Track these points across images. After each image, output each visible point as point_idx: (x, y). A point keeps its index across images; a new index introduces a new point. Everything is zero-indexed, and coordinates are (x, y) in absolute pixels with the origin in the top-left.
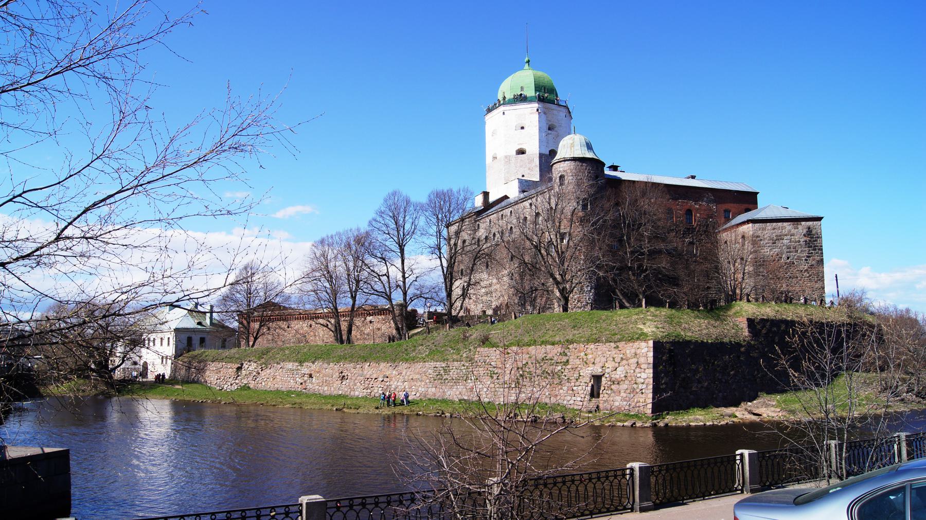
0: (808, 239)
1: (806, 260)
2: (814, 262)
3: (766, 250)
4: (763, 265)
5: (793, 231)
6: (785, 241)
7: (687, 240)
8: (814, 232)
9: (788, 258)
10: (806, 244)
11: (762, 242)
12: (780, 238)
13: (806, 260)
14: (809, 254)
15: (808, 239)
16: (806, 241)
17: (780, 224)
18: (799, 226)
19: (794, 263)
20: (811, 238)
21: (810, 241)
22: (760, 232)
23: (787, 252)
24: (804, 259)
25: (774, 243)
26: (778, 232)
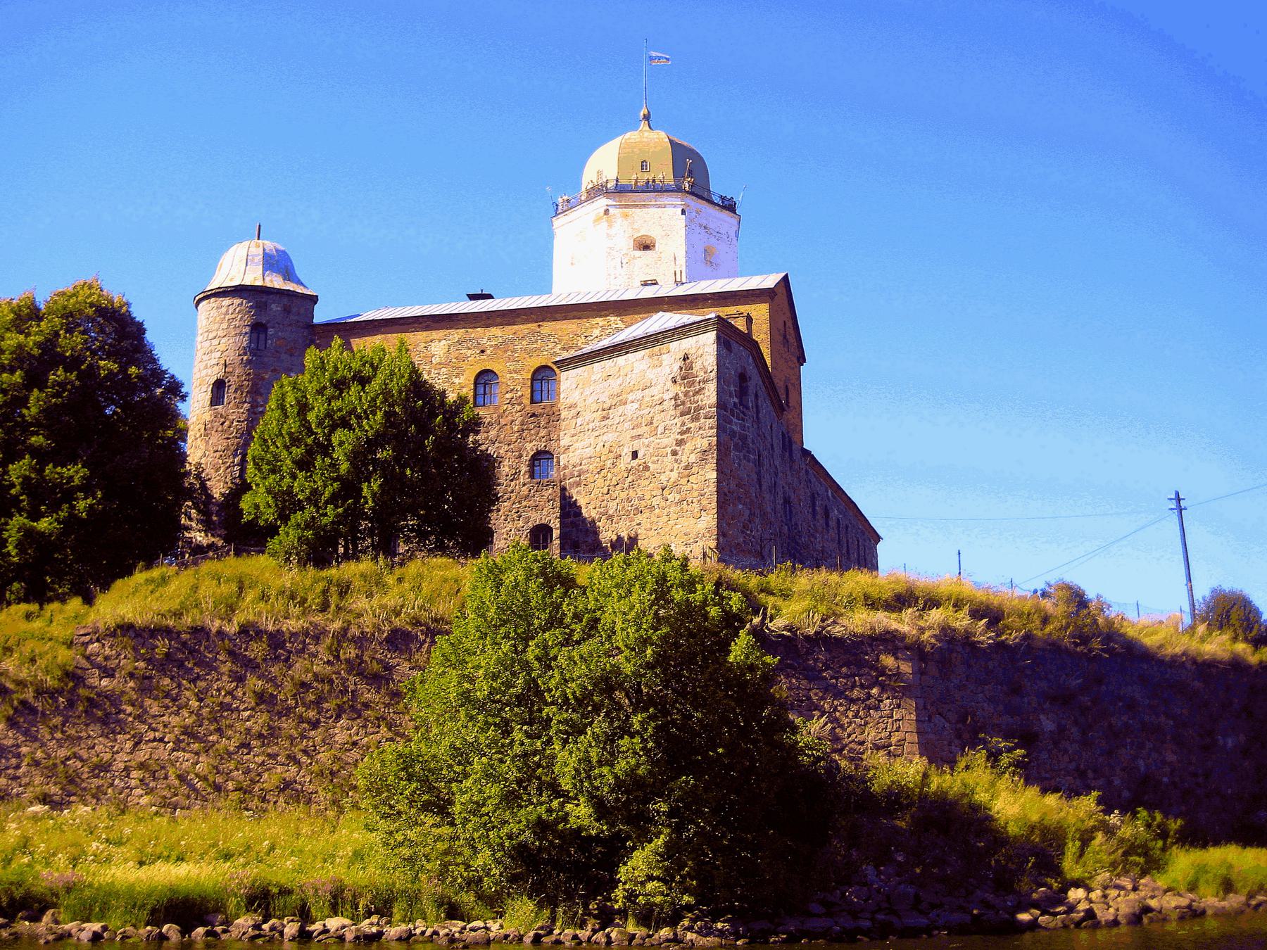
0: (679, 389)
1: (674, 453)
2: (693, 458)
3: (587, 442)
4: (578, 484)
5: (651, 375)
6: (631, 408)
7: (529, 446)
8: (697, 366)
9: (635, 455)
10: (677, 406)
11: (579, 421)
12: (620, 400)
13: (674, 453)
14: (682, 433)
15: (679, 389)
16: (676, 397)
17: (621, 360)
18: (664, 357)
19: (646, 468)
20: (692, 384)
21: (686, 394)
22: (578, 392)
23: (633, 438)
24: (669, 450)
25: (605, 418)
26: (615, 385)
